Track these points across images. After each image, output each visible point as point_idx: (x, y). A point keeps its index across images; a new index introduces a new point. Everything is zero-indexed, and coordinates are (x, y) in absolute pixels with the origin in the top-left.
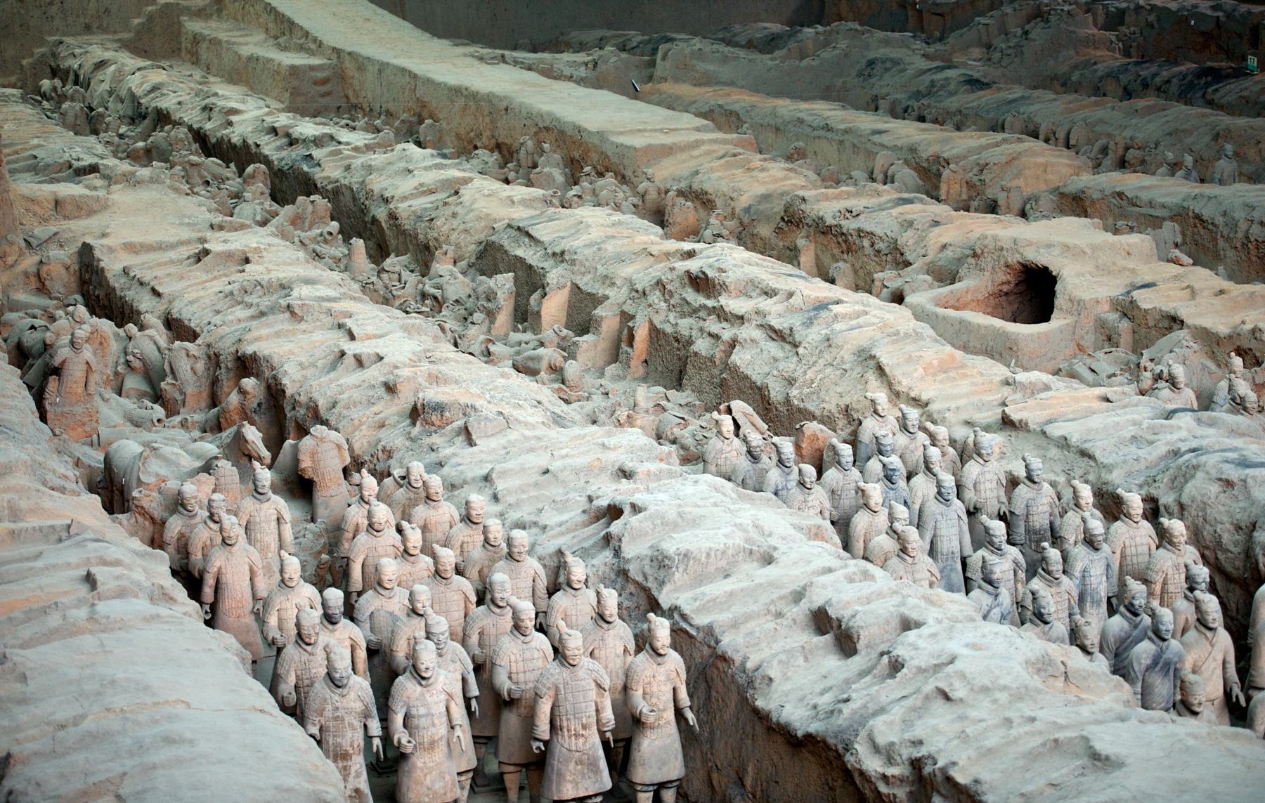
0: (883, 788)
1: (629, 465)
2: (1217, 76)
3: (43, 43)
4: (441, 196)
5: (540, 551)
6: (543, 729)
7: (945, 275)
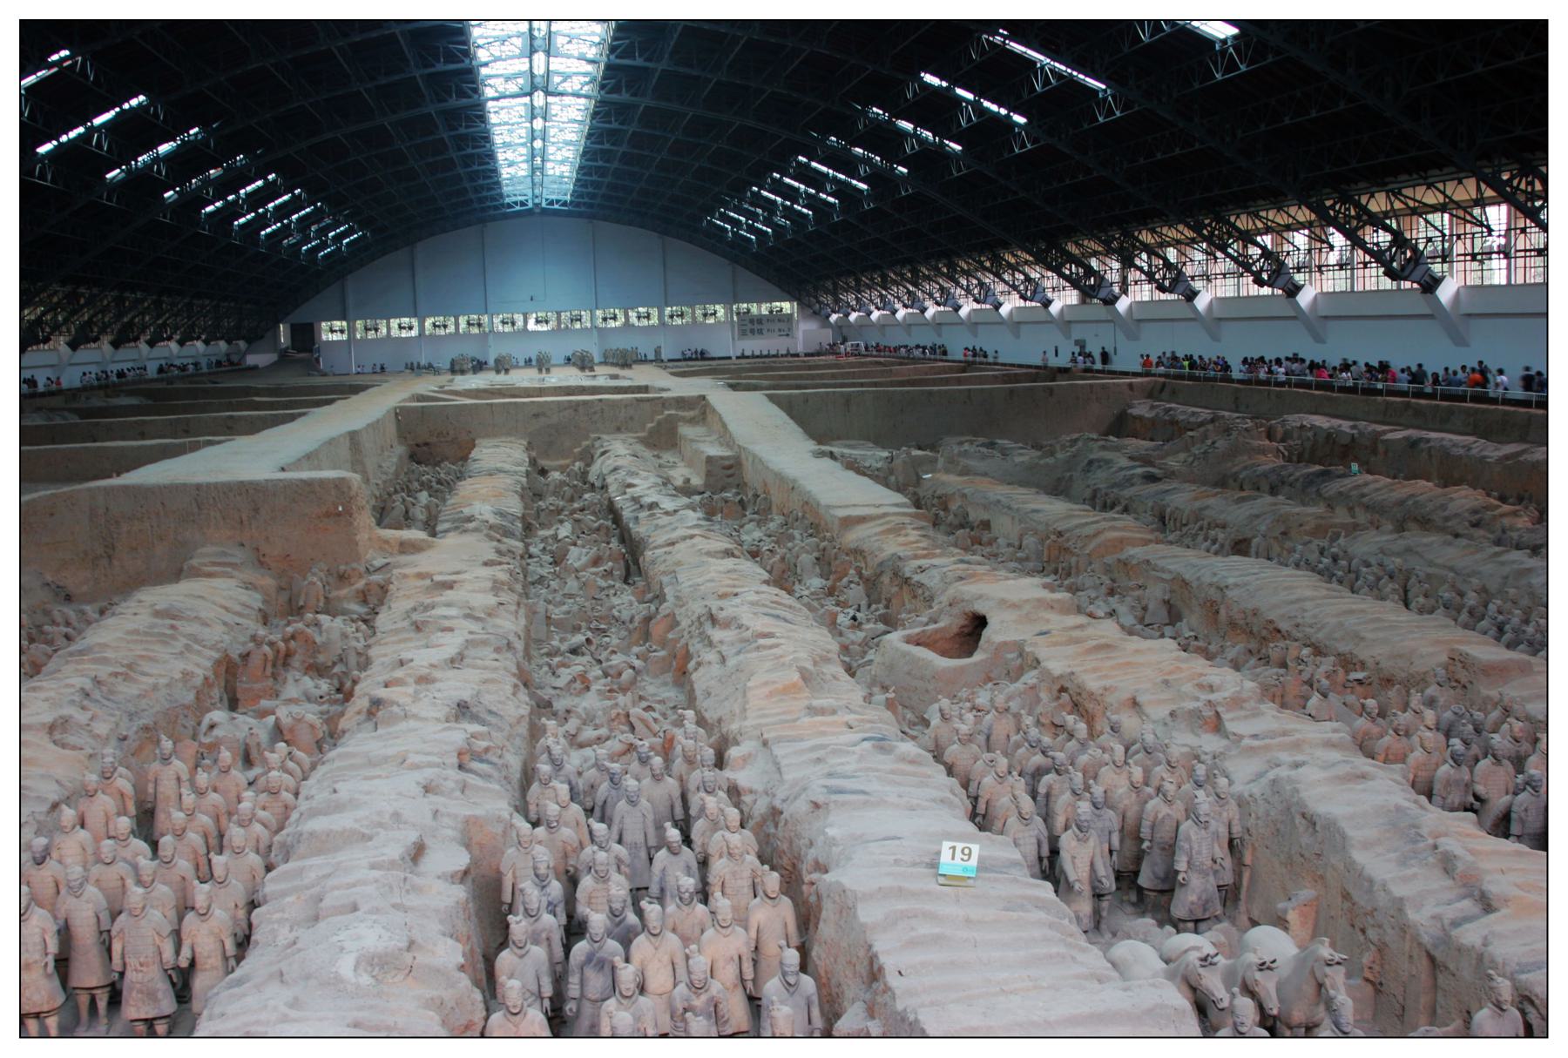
2: (1325, 475)
3: (587, 438)
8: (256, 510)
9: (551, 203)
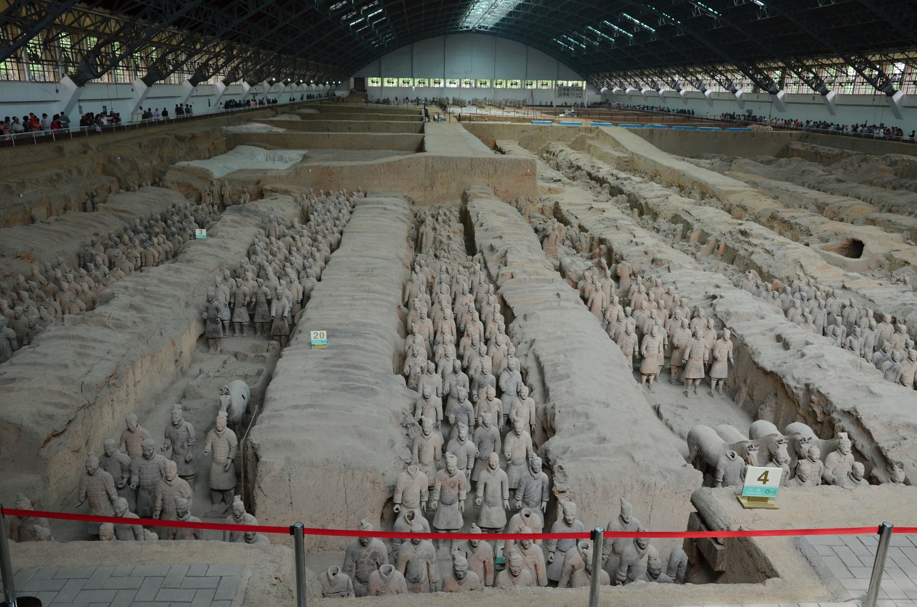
0: (794, 391)
1: (719, 284)
4: (662, 199)
5: (689, 305)
6: (686, 357)
7: (825, 240)
8: (496, 171)
9: (480, 28)
